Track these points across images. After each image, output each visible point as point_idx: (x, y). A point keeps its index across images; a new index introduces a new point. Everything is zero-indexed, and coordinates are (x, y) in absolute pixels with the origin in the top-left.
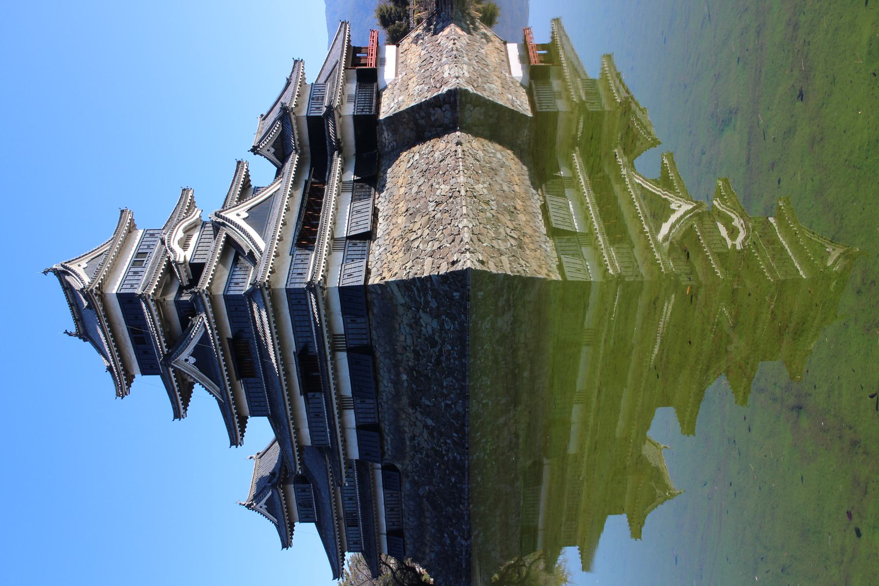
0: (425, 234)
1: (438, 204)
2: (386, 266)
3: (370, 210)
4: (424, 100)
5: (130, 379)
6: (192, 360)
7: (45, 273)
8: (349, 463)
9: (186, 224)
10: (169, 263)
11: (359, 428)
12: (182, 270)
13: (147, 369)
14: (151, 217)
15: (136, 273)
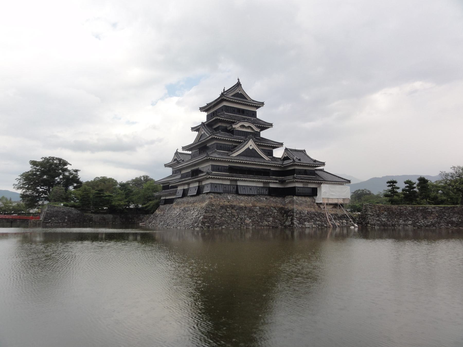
0: (227, 214)
1: (241, 219)
2: (219, 199)
3: (251, 193)
4: (295, 214)
5: (206, 111)
6: (203, 133)
7: (238, 79)
8: (176, 187)
9: (252, 127)
10: (234, 122)
11: (184, 190)
12: (230, 128)
13: (208, 117)
14: (261, 114)
15: (234, 111)
